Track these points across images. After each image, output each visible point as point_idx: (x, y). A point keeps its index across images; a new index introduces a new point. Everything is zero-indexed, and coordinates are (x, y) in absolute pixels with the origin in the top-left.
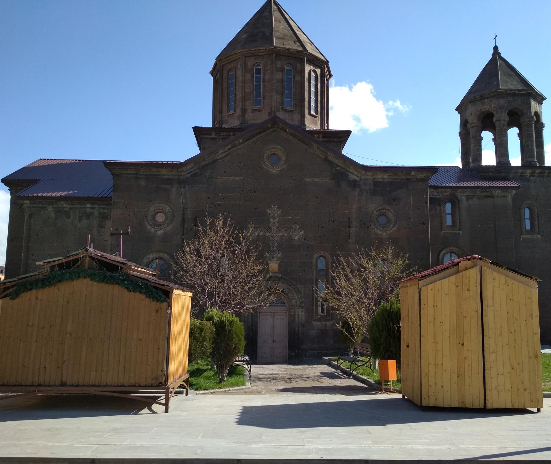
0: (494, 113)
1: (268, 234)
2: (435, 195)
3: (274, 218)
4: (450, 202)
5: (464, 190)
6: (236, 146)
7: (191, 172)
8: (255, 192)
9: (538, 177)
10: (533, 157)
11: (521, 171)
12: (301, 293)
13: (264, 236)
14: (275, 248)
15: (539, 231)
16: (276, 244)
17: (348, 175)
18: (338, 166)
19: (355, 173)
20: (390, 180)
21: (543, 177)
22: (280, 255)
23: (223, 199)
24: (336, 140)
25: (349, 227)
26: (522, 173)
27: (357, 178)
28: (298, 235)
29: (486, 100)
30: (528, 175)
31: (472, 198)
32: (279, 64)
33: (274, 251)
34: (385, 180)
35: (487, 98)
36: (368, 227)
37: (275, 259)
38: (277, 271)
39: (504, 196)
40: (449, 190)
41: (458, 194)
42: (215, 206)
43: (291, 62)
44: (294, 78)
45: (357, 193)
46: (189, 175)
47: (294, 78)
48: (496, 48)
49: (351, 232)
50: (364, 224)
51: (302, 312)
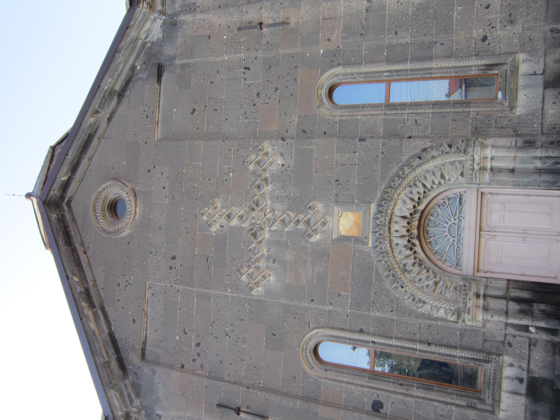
1: (267, 235)
3: (229, 216)
7: (129, 396)
8: (174, 258)
12: (424, 150)
13: (270, 244)
14: (302, 216)
16: (292, 215)
17: (153, 43)
18: (133, 68)
19: (147, 26)
22: (320, 206)
23: (186, 333)
27: (159, 22)
28: (275, 158)
33: (308, 222)
37: (329, 218)
38: (361, 213)
42: (199, 355)
45: (189, 18)
46: (137, 402)
49: (270, 21)
51: (483, 146)
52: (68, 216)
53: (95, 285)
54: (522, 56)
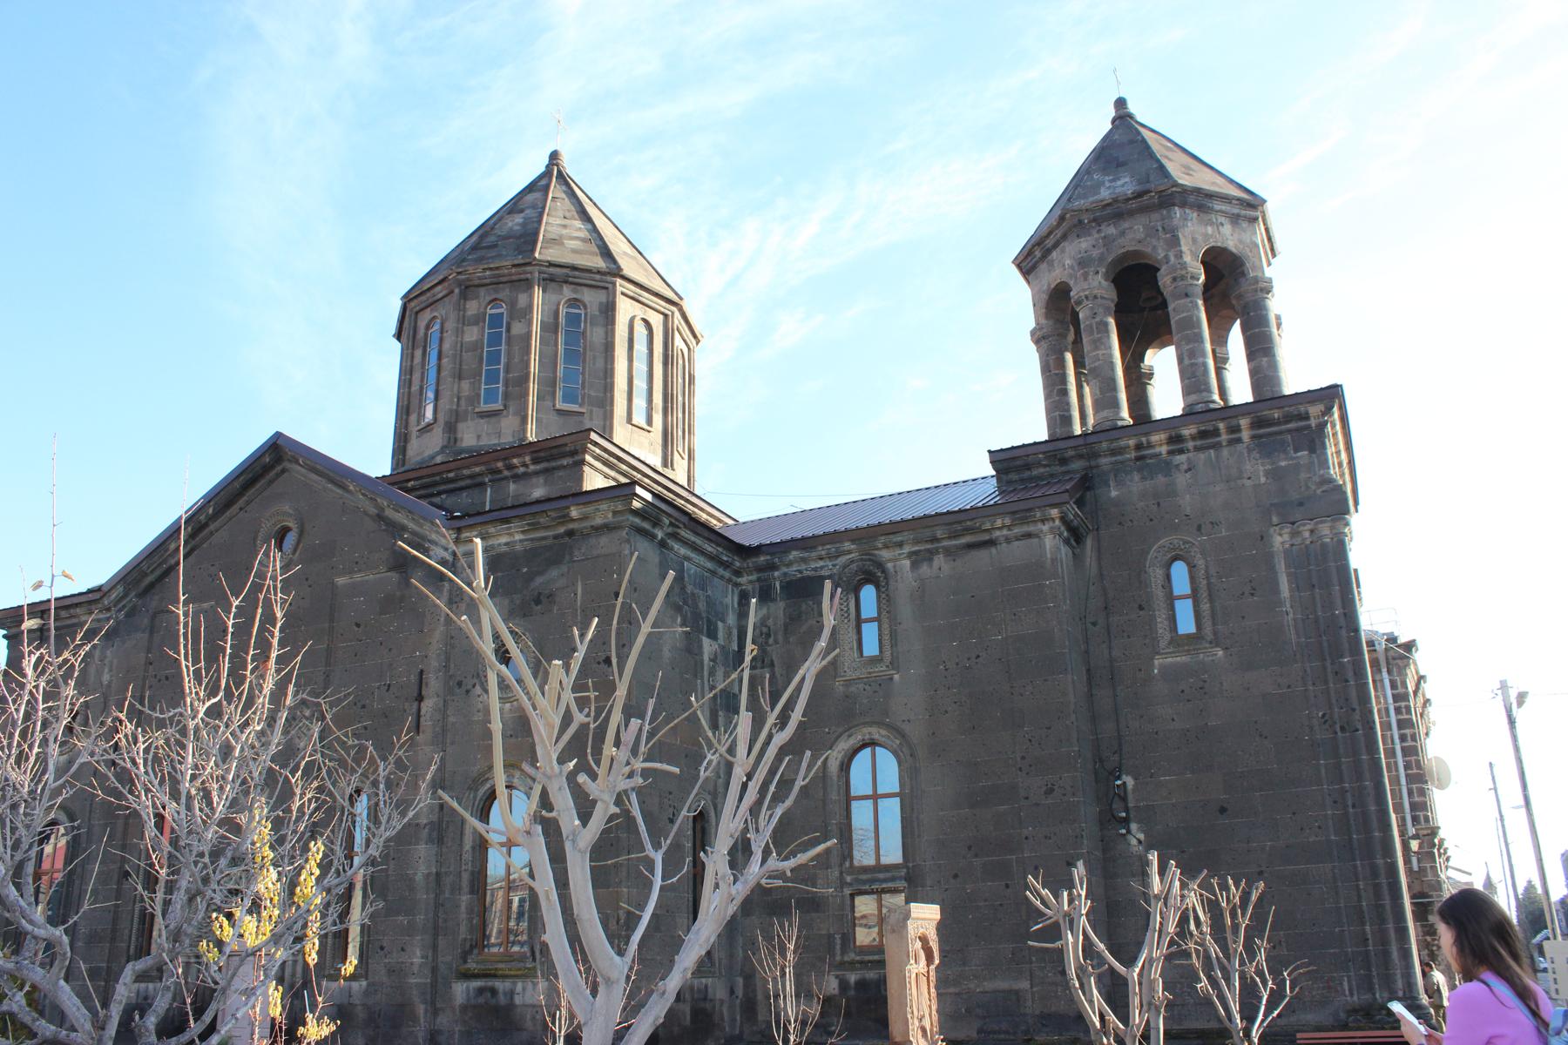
0: (1071, 283)
2: (815, 569)
4: (867, 581)
5: (898, 538)
6: (206, 525)
9: (1197, 449)
10: (1209, 391)
11: (1132, 442)
15: (1215, 633)
20: (528, 545)
21: (1217, 446)
24: (565, 462)
25: (420, 698)
26: (1139, 447)
29: (1054, 254)
30: (1164, 449)
31: (931, 560)
32: (472, 307)
34: (518, 547)
35: (1055, 246)
36: (468, 692)
39: (1029, 535)
40: (847, 545)
41: (885, 554)
43: (499, 296)
44: (508, 330)
47: (508, 330)
48: (1120, 103)
50: (460, 684)
52: (272, 474)
53: (212, 533)
54: (364, 983)
